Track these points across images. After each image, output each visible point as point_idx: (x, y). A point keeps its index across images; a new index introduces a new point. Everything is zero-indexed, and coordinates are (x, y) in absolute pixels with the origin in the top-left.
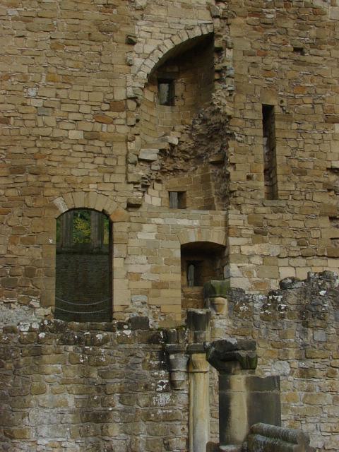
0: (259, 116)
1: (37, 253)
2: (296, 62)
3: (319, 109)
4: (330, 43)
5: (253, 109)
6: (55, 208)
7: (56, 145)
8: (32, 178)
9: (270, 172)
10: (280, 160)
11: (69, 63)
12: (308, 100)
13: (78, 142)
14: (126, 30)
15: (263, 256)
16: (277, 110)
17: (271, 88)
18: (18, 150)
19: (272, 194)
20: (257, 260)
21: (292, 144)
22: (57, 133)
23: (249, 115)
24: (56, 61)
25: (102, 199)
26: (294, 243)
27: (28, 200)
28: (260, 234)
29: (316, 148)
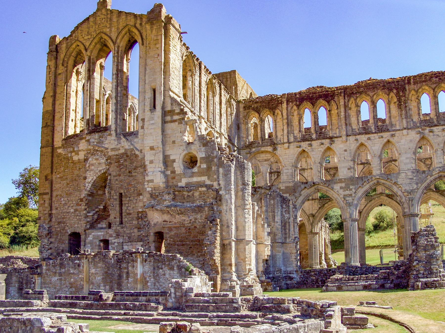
0: (117, 197)
1: (63, 246)
2: (129, 176)
3: (136, 191)
4: (140, 167)
5: (116, 195)
6: (68, 232)
7: (67, 214)
8: (62, 225)
9: (121, 214)
10: (123, 211)
11: (71, 189)
12: (132, 189)
13: (72, 213)
14: (84, 175)
15: (118, 243)
16: (123, 194)
17: (121, 188)
18: (59, 217)
19: (121, 223)
20: (116, 244)
21: (127, 205)
22: (68, 211)
23: (115, 197)
24: (68, 189)
25: (78, 229)
26: (127, 238)
27: (62, 231)
28: (118, 236)
29: (134, 205)
